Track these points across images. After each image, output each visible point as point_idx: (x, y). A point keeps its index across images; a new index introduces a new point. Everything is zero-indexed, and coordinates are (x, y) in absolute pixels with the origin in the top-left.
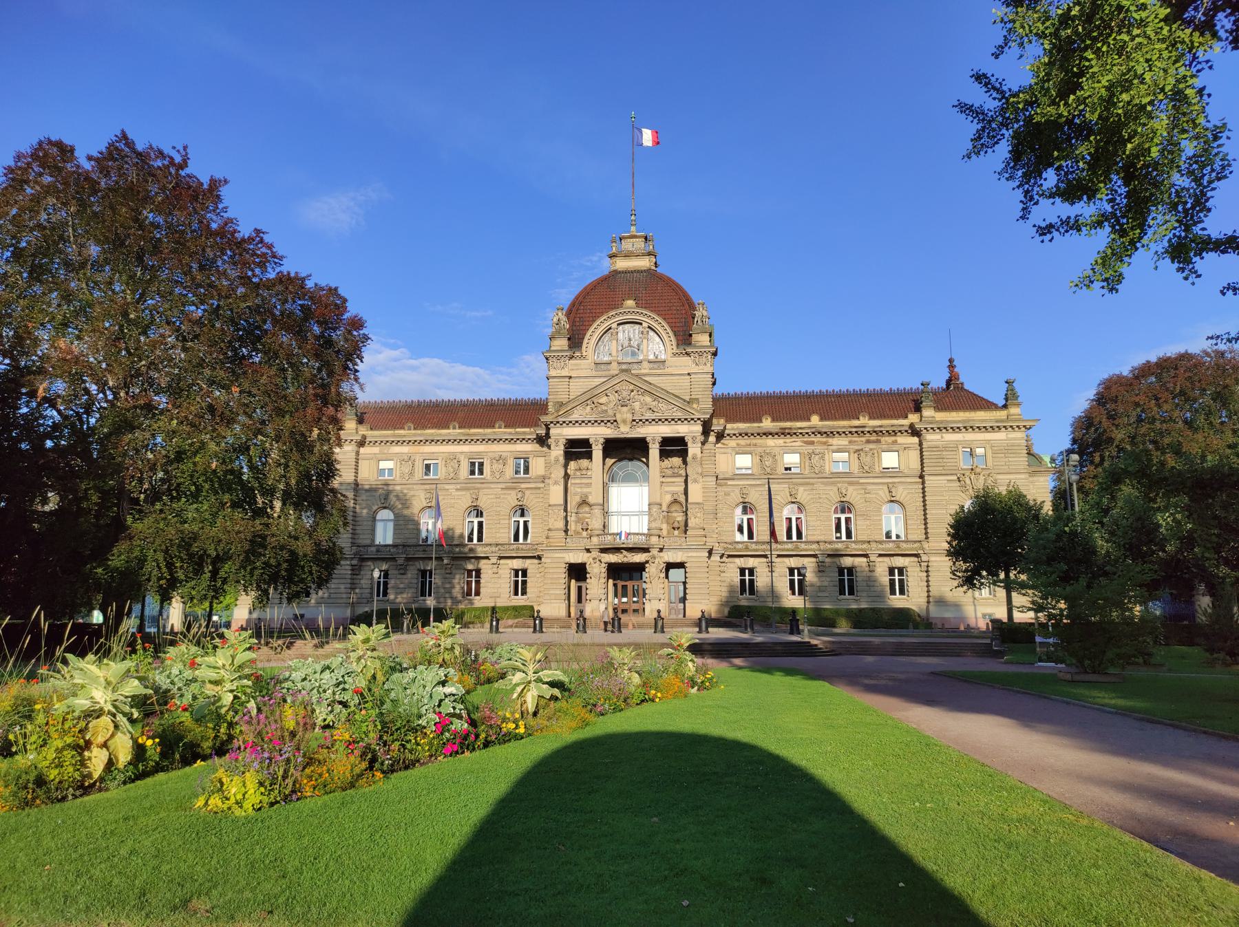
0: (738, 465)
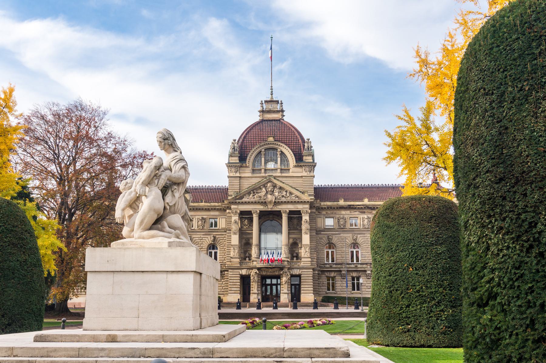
0: (326, 224)
